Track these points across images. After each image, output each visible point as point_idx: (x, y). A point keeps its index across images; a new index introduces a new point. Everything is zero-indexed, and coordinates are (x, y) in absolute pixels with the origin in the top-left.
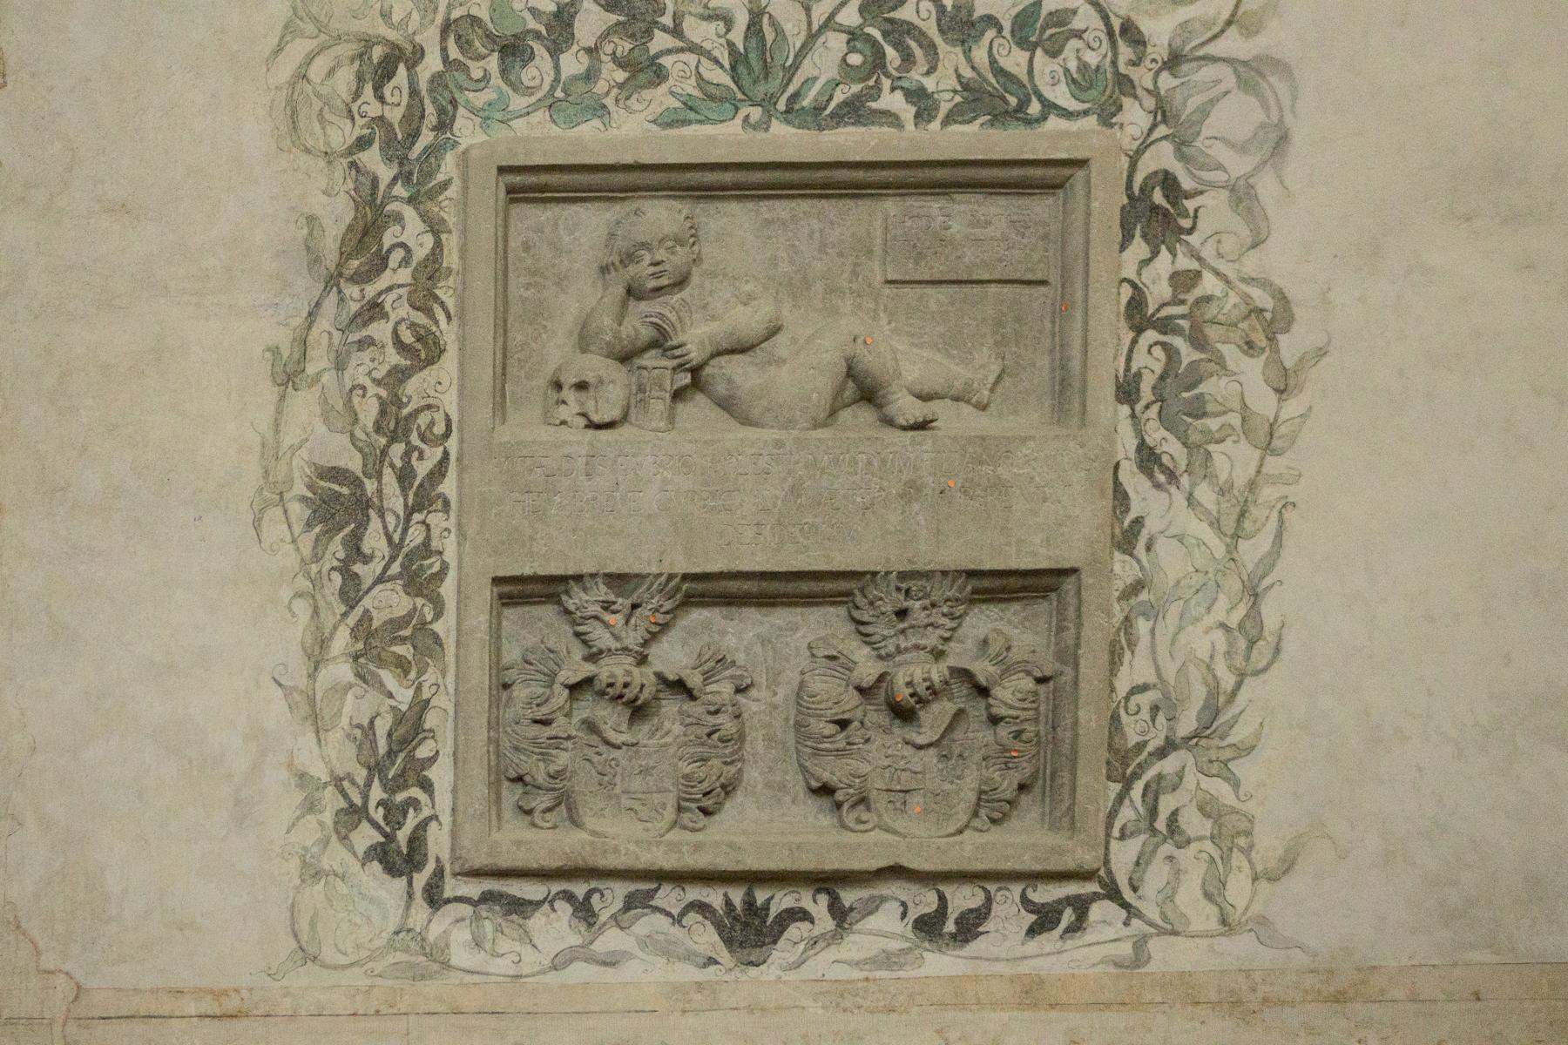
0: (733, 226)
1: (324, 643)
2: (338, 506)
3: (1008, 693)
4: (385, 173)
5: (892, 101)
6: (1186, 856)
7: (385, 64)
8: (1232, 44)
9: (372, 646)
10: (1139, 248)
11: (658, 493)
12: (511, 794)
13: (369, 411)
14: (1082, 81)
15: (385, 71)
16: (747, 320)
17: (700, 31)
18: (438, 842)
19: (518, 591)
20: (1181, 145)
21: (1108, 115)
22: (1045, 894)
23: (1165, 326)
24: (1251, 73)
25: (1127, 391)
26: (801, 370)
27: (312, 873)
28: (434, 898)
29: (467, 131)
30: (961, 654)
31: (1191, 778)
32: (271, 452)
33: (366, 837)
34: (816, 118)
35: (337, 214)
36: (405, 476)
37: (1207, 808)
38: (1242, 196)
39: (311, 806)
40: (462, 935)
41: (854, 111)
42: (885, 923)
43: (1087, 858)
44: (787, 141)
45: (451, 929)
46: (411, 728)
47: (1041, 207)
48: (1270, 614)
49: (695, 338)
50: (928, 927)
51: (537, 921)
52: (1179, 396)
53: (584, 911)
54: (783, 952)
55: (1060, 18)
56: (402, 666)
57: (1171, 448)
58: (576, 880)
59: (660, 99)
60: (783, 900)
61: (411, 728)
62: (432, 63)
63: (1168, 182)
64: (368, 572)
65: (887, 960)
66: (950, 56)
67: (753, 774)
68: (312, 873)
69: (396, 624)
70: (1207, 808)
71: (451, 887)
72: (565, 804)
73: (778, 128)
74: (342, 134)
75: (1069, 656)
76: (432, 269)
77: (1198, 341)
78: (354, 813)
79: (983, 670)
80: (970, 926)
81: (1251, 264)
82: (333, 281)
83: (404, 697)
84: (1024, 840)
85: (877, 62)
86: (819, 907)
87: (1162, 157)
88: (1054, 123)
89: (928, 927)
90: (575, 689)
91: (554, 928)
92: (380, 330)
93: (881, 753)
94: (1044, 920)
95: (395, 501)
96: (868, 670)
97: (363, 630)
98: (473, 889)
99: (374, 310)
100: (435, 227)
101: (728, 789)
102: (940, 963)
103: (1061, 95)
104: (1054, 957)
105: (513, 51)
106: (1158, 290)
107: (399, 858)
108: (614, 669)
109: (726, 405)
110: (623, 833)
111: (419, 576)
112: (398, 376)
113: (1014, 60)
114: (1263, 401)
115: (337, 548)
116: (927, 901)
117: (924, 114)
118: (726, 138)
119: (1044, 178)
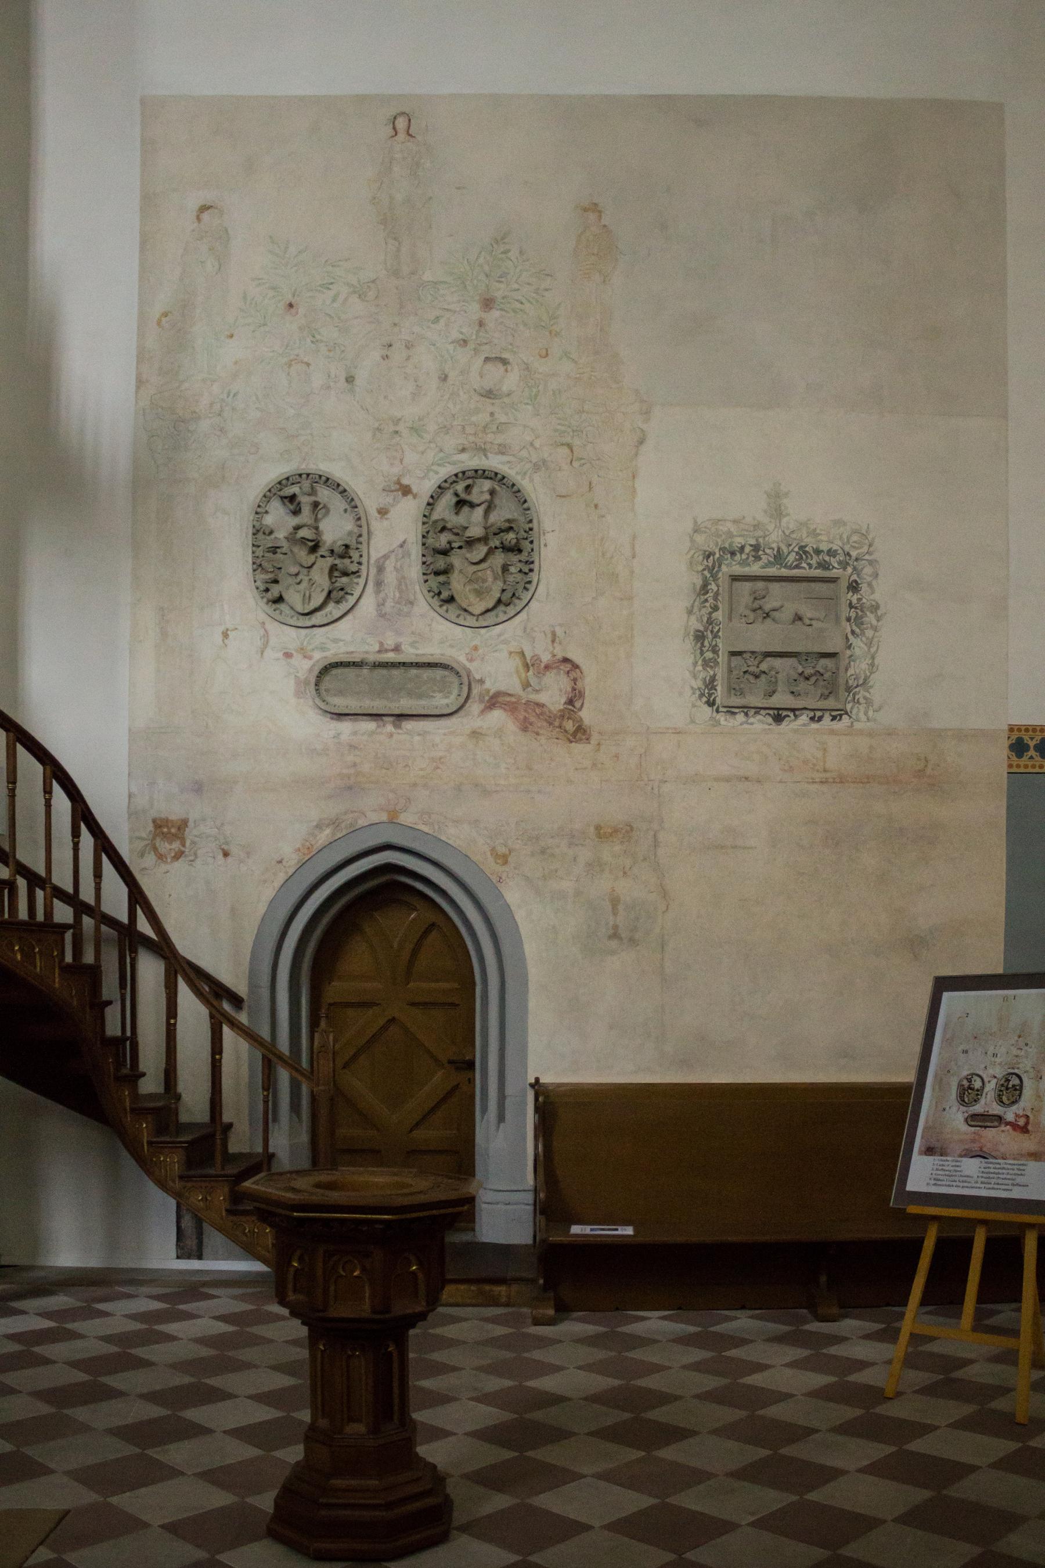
0: (775, 587)
1: (697, 662)
2: (700, 637)
3: (827, 675)
4: (708, 575)
5: (804, 565)
6: (861, 707)
7: (708, 555)
8: (867, 557)
9: (706, 664)
10: (850, 594)
11: (760, 636)
12: (733, 692)
13: (705, 619)
14: (840, 563)
15: (708, 557)
16: (776, 604)
17: (768, 551)
18: (718, 701)
19: (733, 654)
20: (858, 575)
21: (845, 569)
22: (834, 713)
23: (856, 608)
24: (871, 563)
25: (848, 620)
26: (787, 614)
27: (694, 706)
28: (717, 711)
29: (724, 568)
30: (819, 668)
31: (862, 692)
32: (686, 627)
33: (704, 699)
34: (790, 568)
35: (699, 582)
36: (712, 632)
37: (865, 698)
38: (870, 585)
39: (694, 693)
40: (722, 719)
41: (797, 567)
42: (804, 718)
43: (840, 707)
44: (784, 572)
45: (721, 718)
46: (713, 679)
47: (832, 585)
48: (876, 662)
49: (767, 607)
50: (812, 719)
51: (737, 716)
52: (859, 621)
53: (746, 714)
54: (785, 723)
55: (836, 551)
56: (711, 667)
57: (857, 630)
58: (745, 709)
59: (761, 563)
60: (785, 713)
61: (713, 679)
62: (717, 555)
63: (856, 581)
64: (705, 649)
65: (804, 725)
66: (815, 557)
67: (779, 689)
68: (694, 706)
69: (710, 659)
70: (865, 698)
71: (721, 709)
72: (742, 693)
73: (783, 570)
74: (701, 568)
75: (838, 669)
76: (717, 594)
77: (862, 611)
78: (702, 695)
79: (822, 671)
80: (820, 719)
81: (872, 597)
82: (699, 595)
83: (712, 673)
84: (830, 703)
85: (801, 558)
86: (792, 715)
87: (854, 577)
88: (835, 570)
89: (812, 719)
90: (745, 672)
91: (740, 717)
92: (707, 604)
93: (803, 686)
94: (834, 718)
95: (710, 636)
96: (800, 670)
97: (704, 660)
98: (725, 710)
99: (706, 601)
100: (718, 586)
101: (774, 692)
102: (814, 726)
103: (836, 565)
104: (836, 725)
105: (733, 554)
106: (854, 601)
107: (711, 704)
108: (751, 669)
109: (773, 620)
110: (755, 700)
111: (715, 650)
112: (710, 613)
113: (827, 558)
114: (874, 622)
115: (699, 645)
116: (812, 714)
117: (810, 568)
118: (773, 571)
119: (834, 580)
